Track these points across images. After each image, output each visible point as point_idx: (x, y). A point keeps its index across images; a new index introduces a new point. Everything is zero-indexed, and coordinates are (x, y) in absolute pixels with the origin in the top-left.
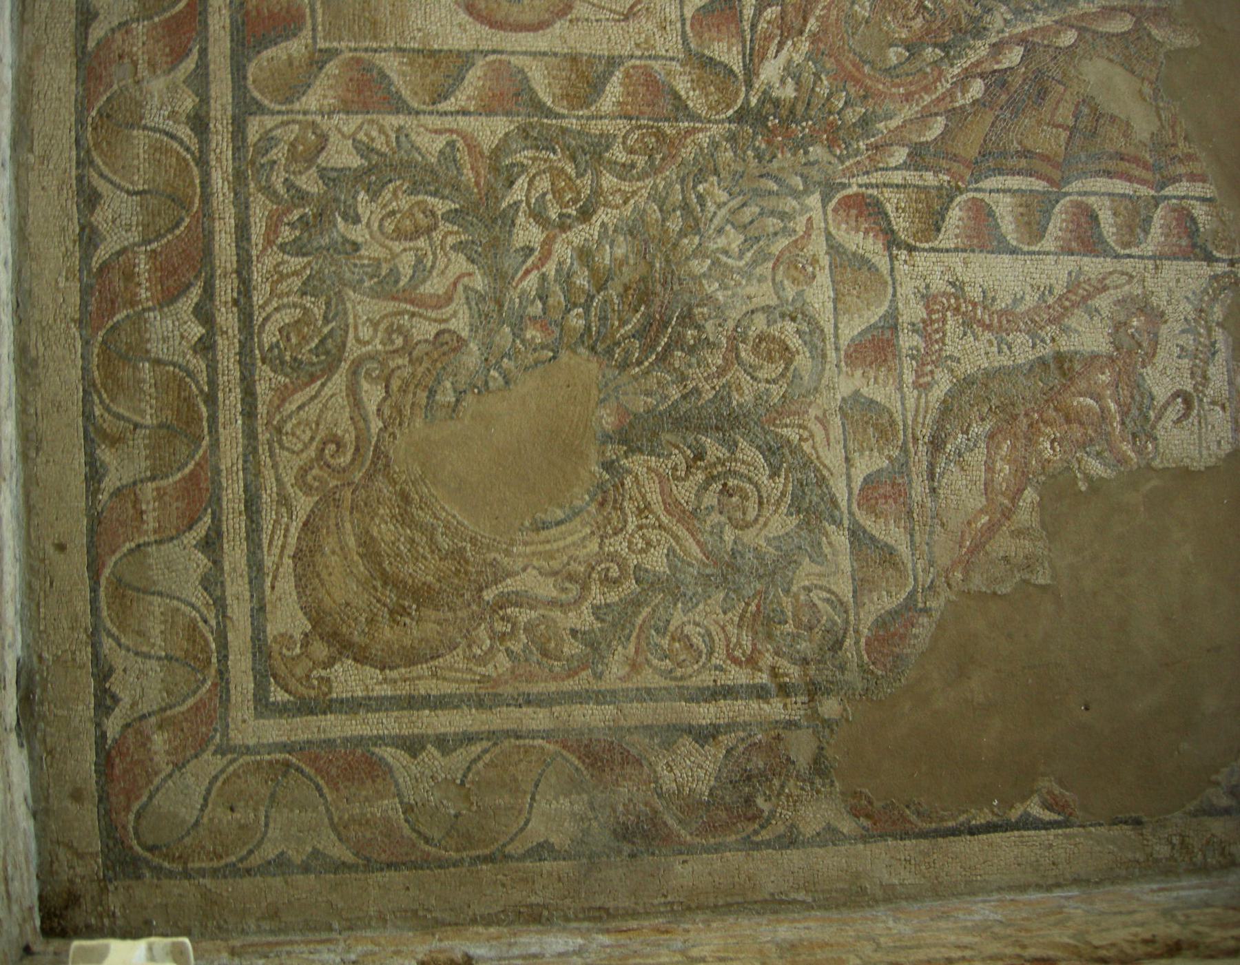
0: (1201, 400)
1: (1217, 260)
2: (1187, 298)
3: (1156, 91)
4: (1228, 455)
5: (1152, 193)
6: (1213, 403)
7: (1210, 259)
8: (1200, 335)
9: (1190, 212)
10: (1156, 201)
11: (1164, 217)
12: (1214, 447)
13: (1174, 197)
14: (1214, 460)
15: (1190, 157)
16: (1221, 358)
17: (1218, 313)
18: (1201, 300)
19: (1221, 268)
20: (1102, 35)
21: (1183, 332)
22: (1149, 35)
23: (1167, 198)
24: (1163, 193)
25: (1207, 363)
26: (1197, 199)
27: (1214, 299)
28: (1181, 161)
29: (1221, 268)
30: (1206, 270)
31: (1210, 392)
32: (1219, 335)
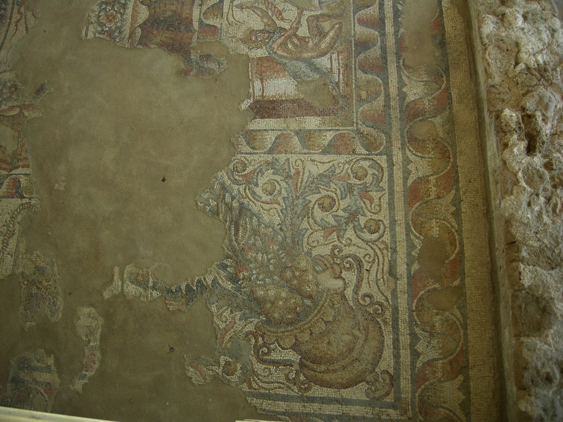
0: (4, 253)
1: (25, 198)
2: (8, 213)
3: (20, 135)
4: (9, 275)
5: (7, 173)
6: (9, 254)
7: (22, 197)
8: (10, 227)
9: (19, 179)
10: (8, 176)
11: (8, 182)
12: (4, 272)
13: (15, 174)
14: (3, 277)
15: (26, 159)
16: (15, 237)
17: (19, 218)
18: (14, 213)
19: (24, 201)
20: (7, 116)
21: (3, 226)
22: (24, 114)
23: (12, 175)
24: (11, 173)
25: (9, 238)
26: (23, 174)
27: (19, 213)
28: (21, 160)
29: (24, 201)
30: (19, 201)
31: (7, 249)
32: (17, 227)
